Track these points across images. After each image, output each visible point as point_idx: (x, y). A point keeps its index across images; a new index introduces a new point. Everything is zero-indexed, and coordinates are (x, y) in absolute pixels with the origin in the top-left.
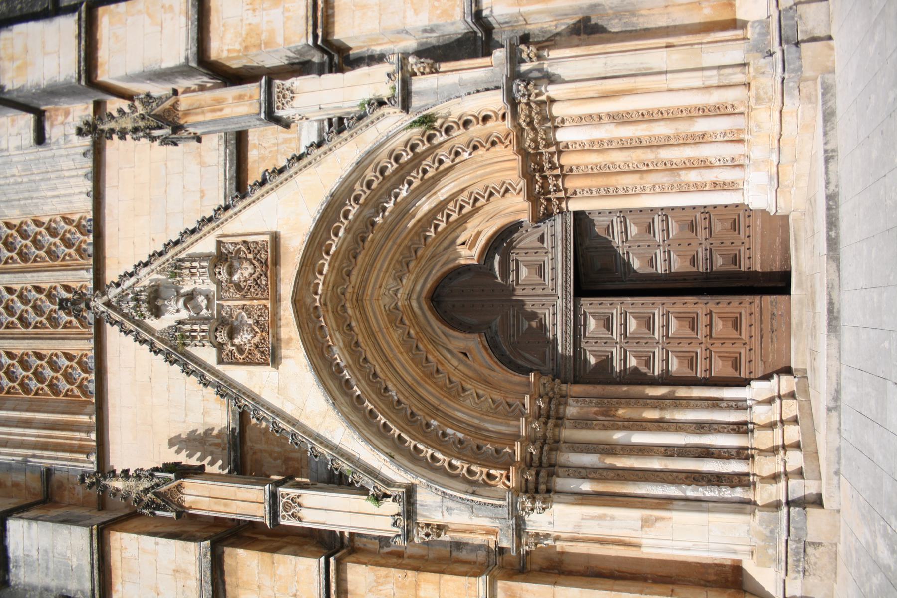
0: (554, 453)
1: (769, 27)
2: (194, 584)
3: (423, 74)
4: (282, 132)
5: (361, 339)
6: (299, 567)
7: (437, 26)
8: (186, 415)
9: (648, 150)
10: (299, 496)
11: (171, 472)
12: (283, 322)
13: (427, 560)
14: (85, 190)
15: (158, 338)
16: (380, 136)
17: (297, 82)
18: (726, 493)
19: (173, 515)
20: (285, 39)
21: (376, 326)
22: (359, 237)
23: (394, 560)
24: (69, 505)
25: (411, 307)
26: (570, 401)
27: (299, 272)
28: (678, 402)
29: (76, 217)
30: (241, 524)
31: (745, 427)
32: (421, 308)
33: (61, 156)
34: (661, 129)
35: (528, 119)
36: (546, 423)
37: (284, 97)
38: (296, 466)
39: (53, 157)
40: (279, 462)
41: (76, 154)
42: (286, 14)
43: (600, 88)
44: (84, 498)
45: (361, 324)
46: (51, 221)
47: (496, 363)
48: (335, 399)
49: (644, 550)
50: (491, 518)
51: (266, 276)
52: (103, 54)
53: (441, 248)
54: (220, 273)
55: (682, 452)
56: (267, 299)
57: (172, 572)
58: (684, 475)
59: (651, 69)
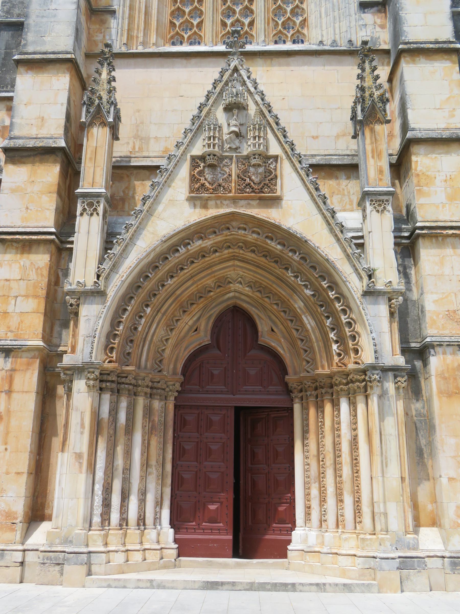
0: (127, 392)
1: (414, 549)
2: (34, 132)
4: (358, 198)
5: (207, 259)
7: (424, 316)
9: (332, 461)
10: (98, 214)
11: (114, 119)
13: (53, 302)
14: (324, 39)
15: (210, 110)
16: (346, 276)
18: (98, 510)
19: (83, 120)
20: (422, 205)
21: (216, 269)
22: (277, 259)
23: (53, 280)
24: (89, 29)
25: (230, 292)
26: (163, 403)
28: (160, 477)
29: (305, 31)
30: (76, 166)
31: (142, 524)
32: (229, 299)
33: (350, 22)
34: (346, 471)
35: (354, 380)
36: (147, 386)
39: (350, 15)
40: (122, 194)
42: (441, 205)
43: (374, 431)
44: (94, 41)
45: (217, 259)
46: (303, 9)
47: (190, 351)
48: (165, 242)
49: (60, 454)
50: (83, 350)
51: (251, 192)
53: (271, 314)
54: (255, 158)
55: (126, 481)
59: (386, 466)
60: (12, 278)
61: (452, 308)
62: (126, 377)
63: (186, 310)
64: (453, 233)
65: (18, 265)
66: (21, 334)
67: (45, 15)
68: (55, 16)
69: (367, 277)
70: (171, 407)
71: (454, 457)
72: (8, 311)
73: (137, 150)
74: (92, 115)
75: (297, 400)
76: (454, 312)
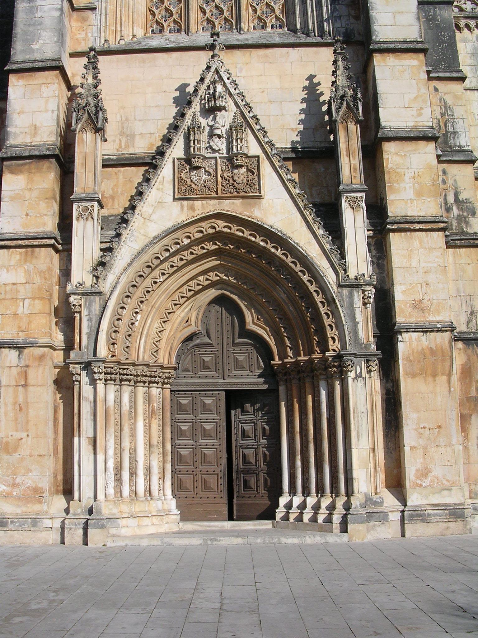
2: (28, 140)
16: (324, 270)
20: (392, 201)
28: (161, 455)
38: (110, 204)
40: (111, 192)
42: (409, 202)
50: (88, 346)
52: (391, 60)
54: (237, 160)
55: (133, 460)
58: (119, 460)
61: (418, 297)
64: (420, 228)
67: (32, 23)
68: (41, 24)
70: (167, 392)
71: (416, 429)
73: (123, 147)
75: (281, 383)
76: (420, 301)
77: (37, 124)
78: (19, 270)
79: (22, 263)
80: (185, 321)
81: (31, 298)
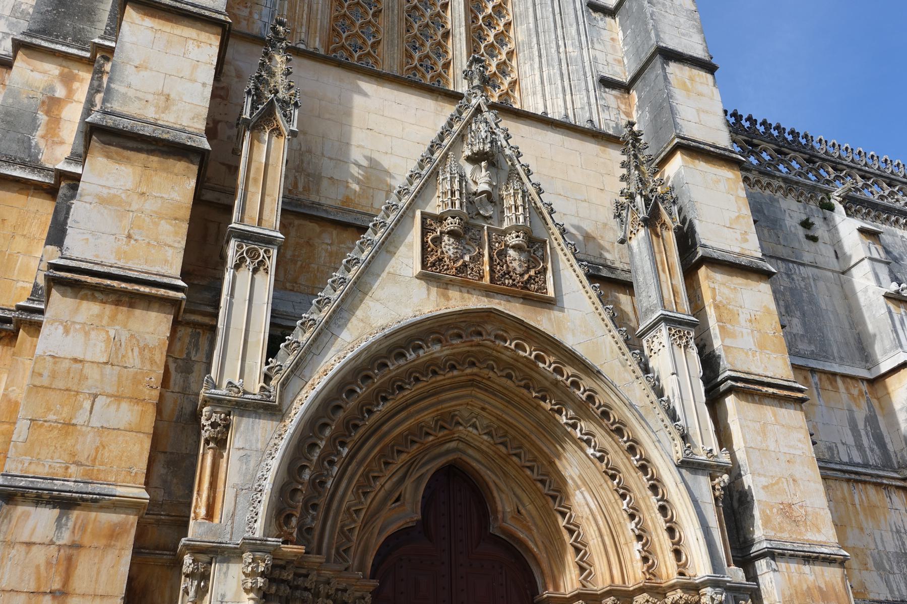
2: (150, 113)
3: (714, 488)
5: (439, 378)
6: (170, 252)
8: (331, 159)
12: (466, 295)
17: (694, 352)
19: (246, 115)
21: (444, 397)
27: (521, 322)
32: (448, 452)
37: (680, 338)
41: (591, 113)
42: (750, 353)
51: (514, 285)
53: (513, 485)
54: (517, 236)
56: (492, 280)
57: (166, 91)
60: (88, 357)
61: (787, 500)
62: (306, 576)
63: (391, 461)
65: (103, 335)
66: (98, 470)
69: (681, 439)
72: (74, 421)
73: (301, 189)
74: (259, 113)
77: (172, 96)
78: (93, 334)
79: (104, 322)
80: (394, 498)
81: (112, 396)
